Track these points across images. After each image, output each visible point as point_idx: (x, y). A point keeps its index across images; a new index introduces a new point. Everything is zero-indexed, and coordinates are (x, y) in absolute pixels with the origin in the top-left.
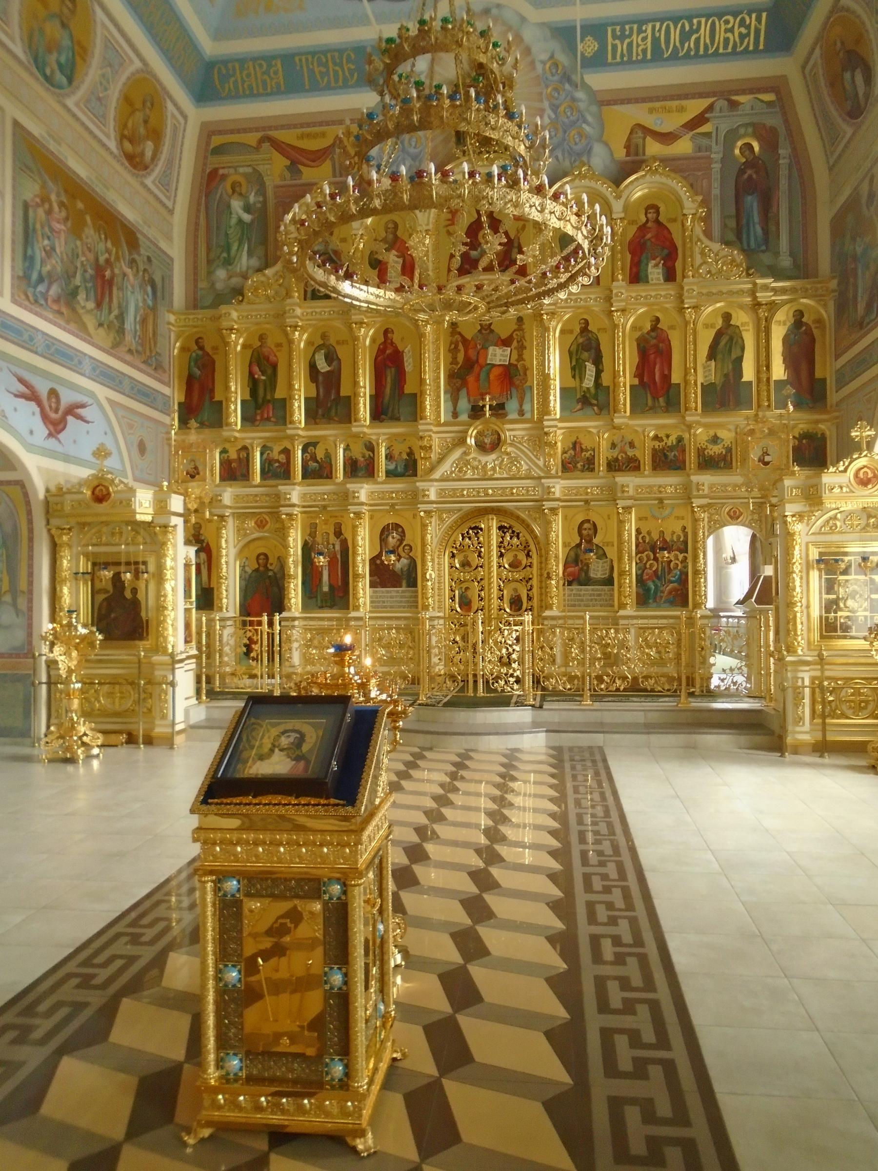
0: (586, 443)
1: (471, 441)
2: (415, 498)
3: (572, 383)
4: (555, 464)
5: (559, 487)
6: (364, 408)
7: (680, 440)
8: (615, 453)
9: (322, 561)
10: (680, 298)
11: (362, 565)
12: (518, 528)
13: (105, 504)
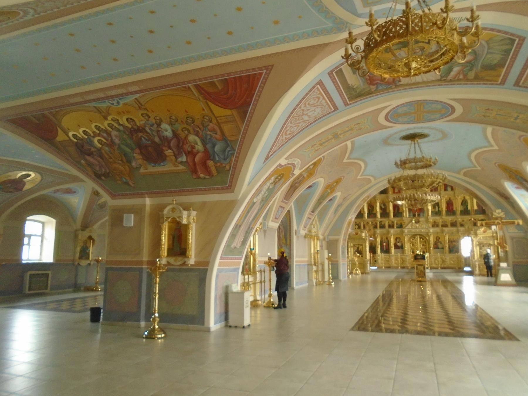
0: (437, 221)
1: (414, 222)
2: (402, 232)
3: (433, 210)
4: (430, 225)
5: (431, 230)
6: (392, 215)
7: (456, 221)
8: (443, 224)
9: (385, 244)
10: (454, 193)
11: (392, 245)
12: (423, 238)
13: (358, 235)
